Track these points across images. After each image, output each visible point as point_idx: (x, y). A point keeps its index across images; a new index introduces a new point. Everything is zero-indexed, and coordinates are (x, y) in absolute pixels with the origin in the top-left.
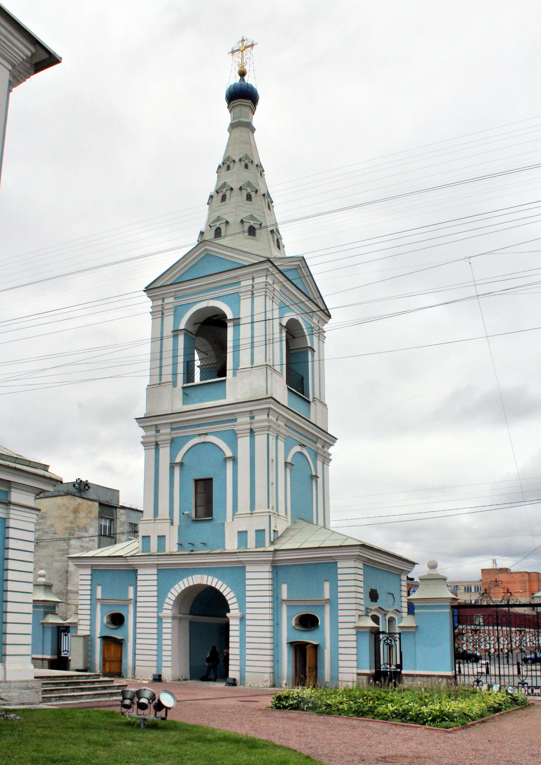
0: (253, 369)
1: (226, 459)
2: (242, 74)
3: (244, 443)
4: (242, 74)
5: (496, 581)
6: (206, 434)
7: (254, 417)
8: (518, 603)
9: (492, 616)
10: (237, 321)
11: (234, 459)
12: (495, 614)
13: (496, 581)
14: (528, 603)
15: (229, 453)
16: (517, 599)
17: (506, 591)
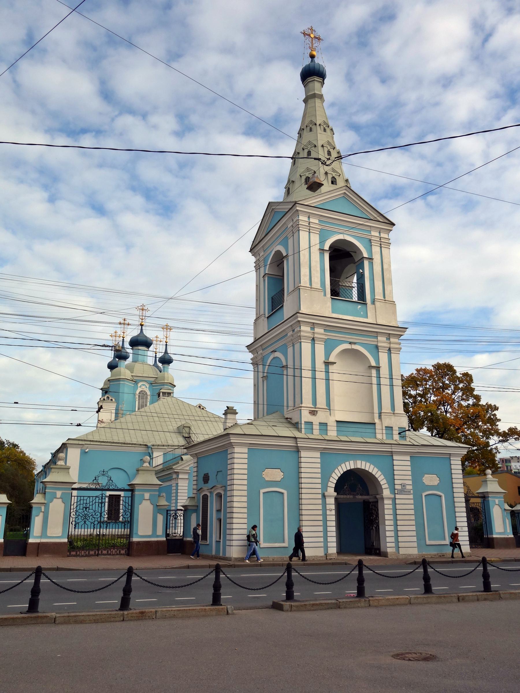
0: (386, 302)
1: (371, 367)
2: (312, 57)
3: (383, 357)
4: (312, 57)
5: (104, 472)
6: (355, 343)
7: (390, 338)
8: (116, 488)
9: (98, 497)
10: (370, 259)
11: (378, 368)
12: (101, 496)
13: (104, 472)
14: (123, 488)
15: (373, 364)
16: (116, 485)
17: (109, 479)
